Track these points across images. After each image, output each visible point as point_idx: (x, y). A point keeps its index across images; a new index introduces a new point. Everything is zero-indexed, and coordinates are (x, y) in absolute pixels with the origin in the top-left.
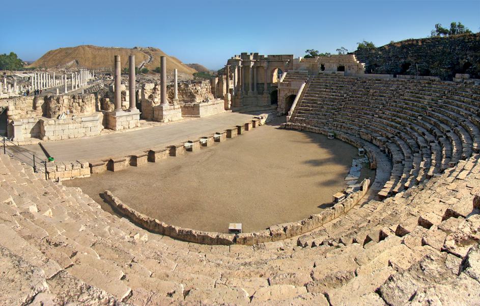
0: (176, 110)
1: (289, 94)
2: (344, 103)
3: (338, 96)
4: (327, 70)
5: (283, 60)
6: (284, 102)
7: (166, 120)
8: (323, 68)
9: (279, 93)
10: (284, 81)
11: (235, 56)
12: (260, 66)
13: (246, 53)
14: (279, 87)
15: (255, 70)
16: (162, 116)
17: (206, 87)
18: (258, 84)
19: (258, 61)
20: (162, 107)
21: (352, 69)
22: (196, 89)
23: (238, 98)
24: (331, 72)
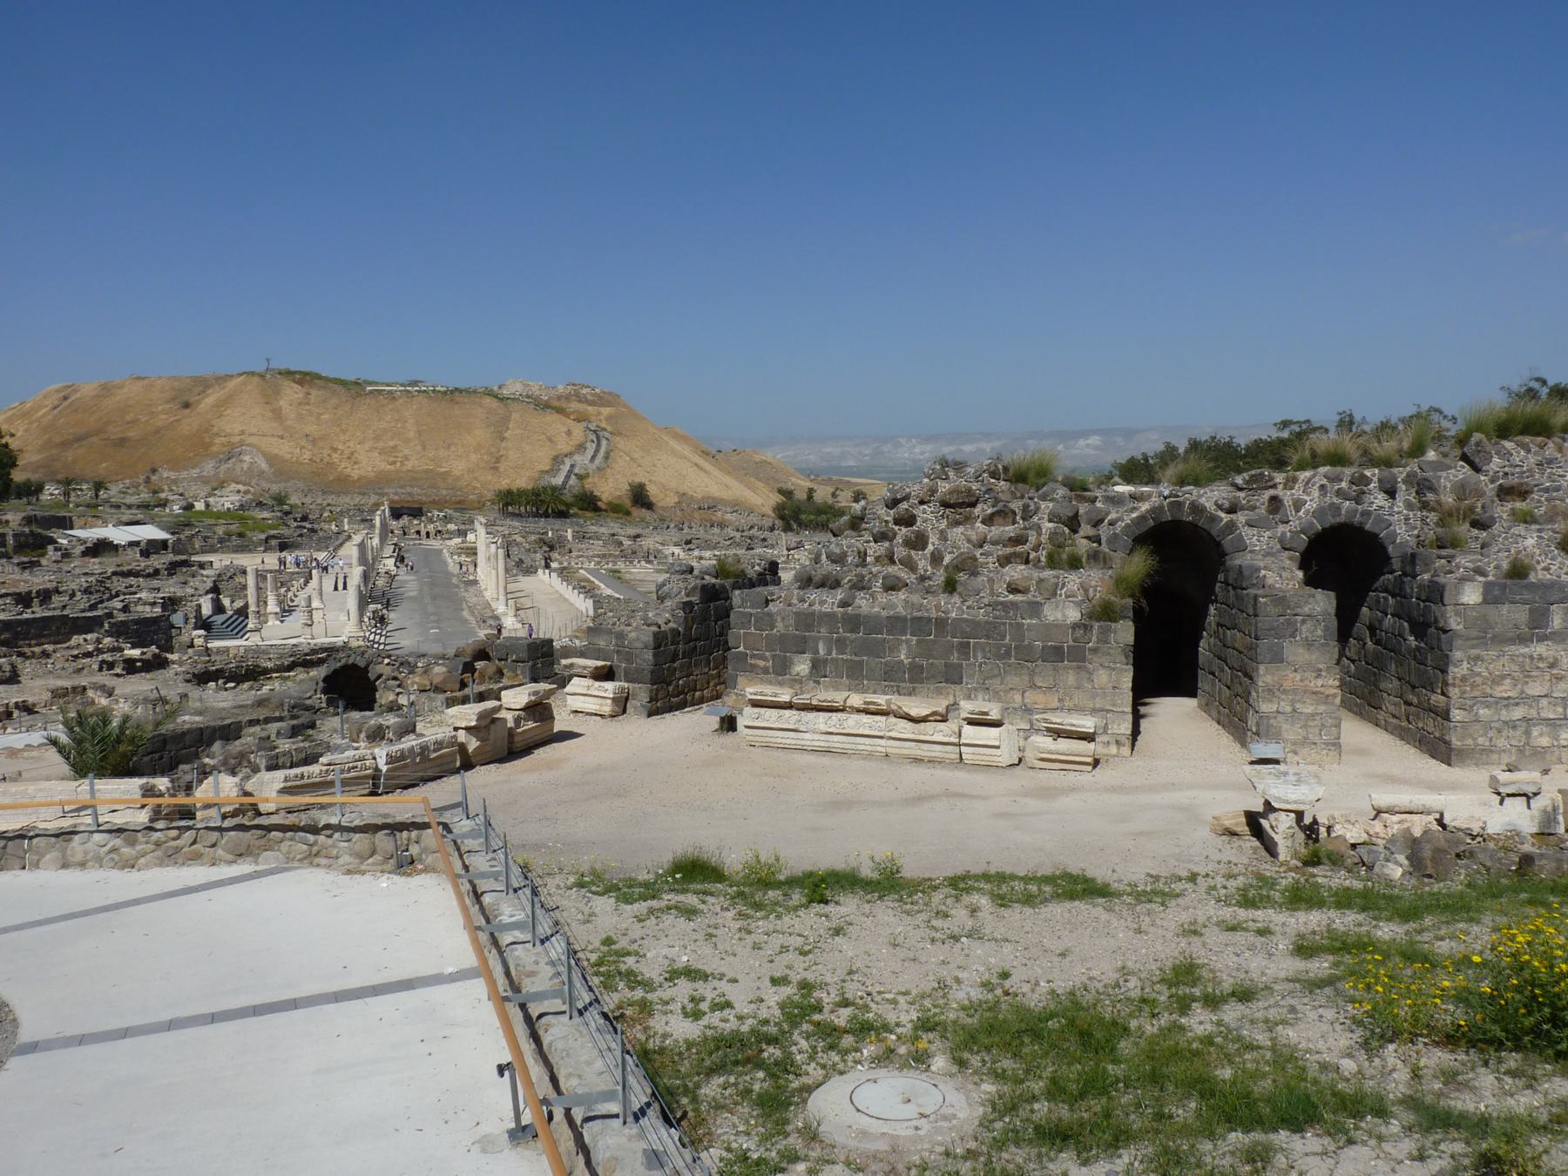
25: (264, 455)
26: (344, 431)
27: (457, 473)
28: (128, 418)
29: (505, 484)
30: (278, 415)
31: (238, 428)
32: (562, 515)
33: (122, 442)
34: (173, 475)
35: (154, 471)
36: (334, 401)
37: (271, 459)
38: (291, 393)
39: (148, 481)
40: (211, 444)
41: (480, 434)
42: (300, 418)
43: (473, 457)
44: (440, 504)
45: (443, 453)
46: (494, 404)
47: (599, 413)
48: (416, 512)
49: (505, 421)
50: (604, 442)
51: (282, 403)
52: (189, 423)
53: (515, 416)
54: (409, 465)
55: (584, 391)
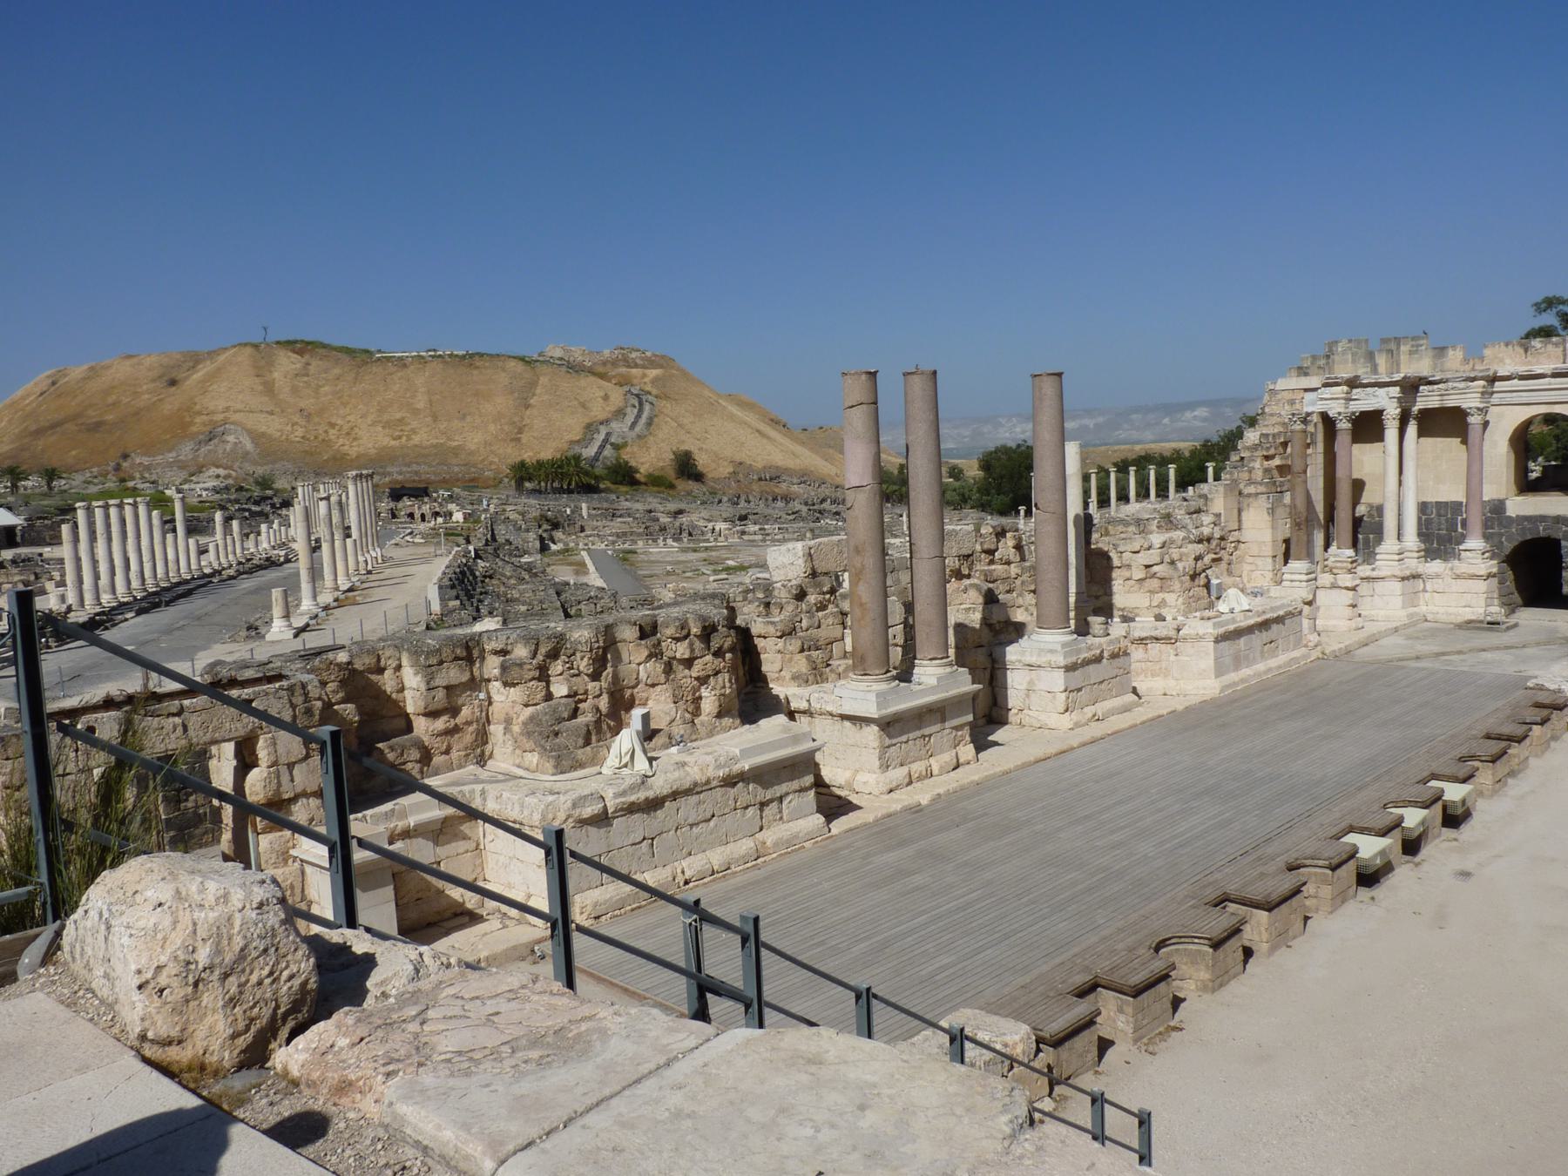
15: (1412, 429)
18: (1423, 507)
25: (250, 432)
26: (345, 405)
27: (473, 447)
28: (110, 400)
29: (528, 456)
30: (269, 389)
31: (221, 404)
32: (589, 490)
33: (97, 427)
34: (146, 460)
35: (125, 457)
36: (337, 371)
37: (257, 437)
38: (287, 363)
39: (118, 468)
40: (192, 423)
41: (502, 403)
42: (295, 390)
43: (492, 428)
44: (446, 483)
45: (456, 424)
46: (520, 367)
47: (645, 375)
48: (420, 493)
49: (533, 384)
50: (647, 407)
51: (276, 375)
52: (173, 402)
53: (543, 380)
54: (416, 439)
55: (634, 355)
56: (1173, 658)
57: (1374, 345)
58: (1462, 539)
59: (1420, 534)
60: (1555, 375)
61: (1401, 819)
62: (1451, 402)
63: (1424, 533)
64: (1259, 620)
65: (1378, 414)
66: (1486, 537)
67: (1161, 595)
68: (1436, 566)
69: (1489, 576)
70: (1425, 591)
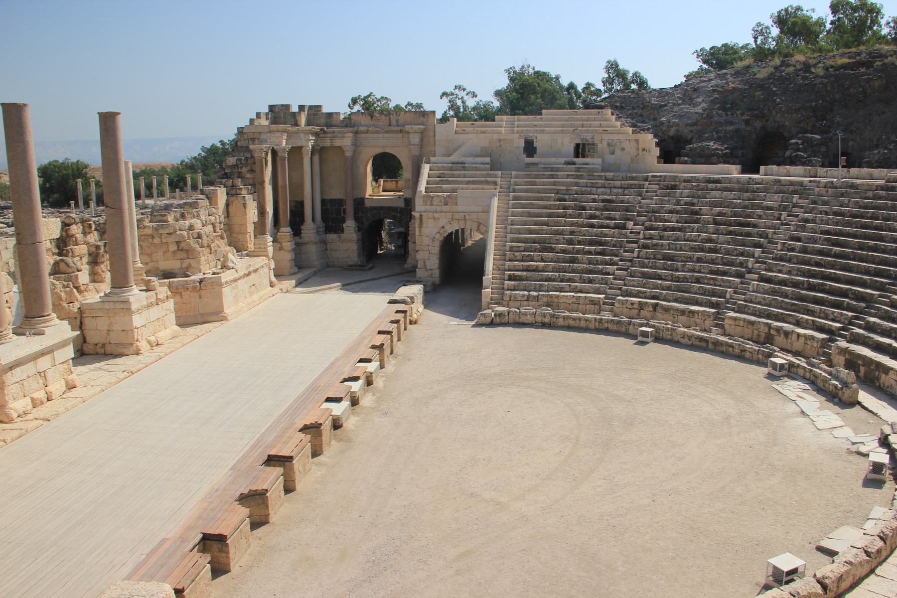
0: (161, 305)
1: (450, 229)
2: (635, 245)
3: (608, 227)
4: (543, 156)
5: (408, 128)
6: (436, 249)
7: (143, 345)
8: (530, 148)
9: (421, 226)
10: (427, 190)
11: (258, 115)
12: (332, 147)
13: (287, 107)
14: (419, 206)
16: (128, 331)
17: (212, 218)
18: (323, 202)
19: (325, 132)
20: (127, 302)
21: (618, 152)
22: (191, 228)
23: (281, 249)
24: (563, 160)
56: (198, 300)
57: (295, 109)
58: (343, 221)
59: (323, 218)
60: (387, 132)
61: (351, 387)
62: (337, 145)
63: (324, 218)
64: (246, 272)
65: (301, 148)
66: (357, 219)
67: (188, 261)
68: (332, 237)
69: (358, 241)
70: (326, 249)
